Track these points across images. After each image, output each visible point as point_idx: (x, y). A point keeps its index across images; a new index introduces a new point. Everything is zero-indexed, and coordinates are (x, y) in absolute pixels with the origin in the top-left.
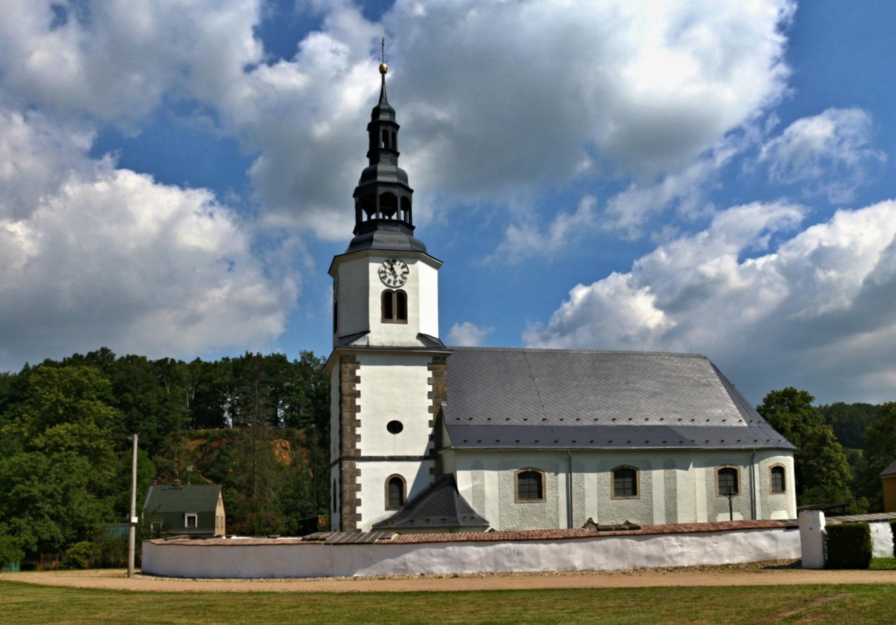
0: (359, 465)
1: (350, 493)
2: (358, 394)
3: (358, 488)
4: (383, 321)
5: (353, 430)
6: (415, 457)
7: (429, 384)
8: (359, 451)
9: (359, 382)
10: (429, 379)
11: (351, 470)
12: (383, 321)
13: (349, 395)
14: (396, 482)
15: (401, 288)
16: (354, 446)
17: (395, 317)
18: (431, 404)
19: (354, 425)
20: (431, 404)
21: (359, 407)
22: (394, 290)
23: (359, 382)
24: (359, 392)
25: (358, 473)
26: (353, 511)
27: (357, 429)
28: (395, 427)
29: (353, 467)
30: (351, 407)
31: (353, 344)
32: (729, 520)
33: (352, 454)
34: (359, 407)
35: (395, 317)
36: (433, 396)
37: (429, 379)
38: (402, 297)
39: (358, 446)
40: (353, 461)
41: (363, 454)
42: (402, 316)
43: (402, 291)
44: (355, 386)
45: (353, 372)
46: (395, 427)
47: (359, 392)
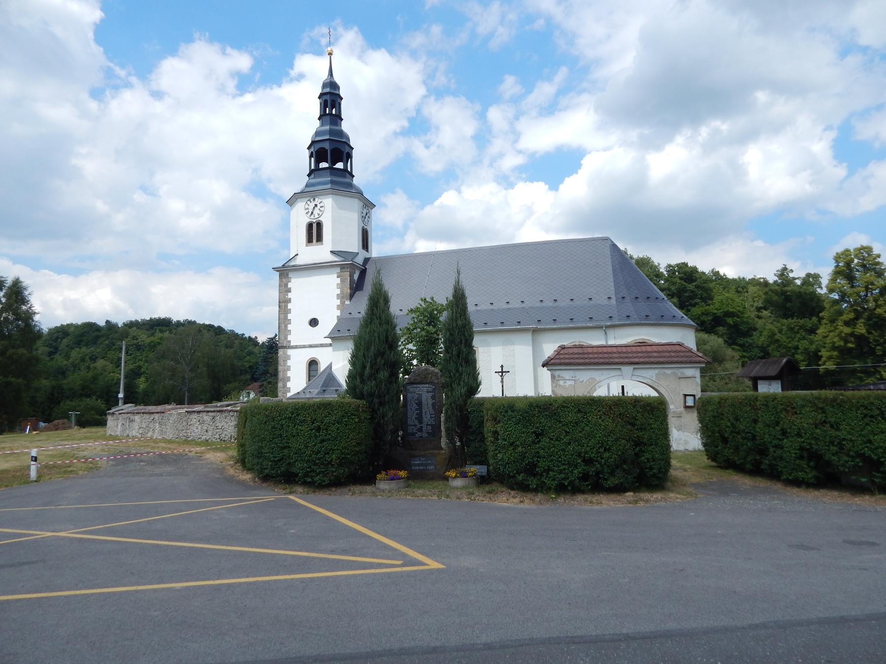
0: (290, 352)
1: (283, 373)
2: (289, 301)
3: (289, 368)
4: (307, 246)
5: (286, 326)
6: (326, 344)
7: (338, 288)
8: (290, 342)
9: (290, 292)
10: (338, 284)
11: (284, 356)
12: (307, 246)
13: (283, 302)
14: (313, 364)
15: (319, 219)
16: (286, 338)
17: (314, 240)
18: (339, 304)
19: (287, 323)
20: (339, 304)
21: (290, 309)
22: (314, 221)
23: (290, 292)
24: (290, 299)
25: (289, 357)
26: (285, 386)
27: (289, 325)
28: (314, 322)
29: (285, 354)
30: (285, 310)
31: (286, 265)
32: (501, 395)
33: (285, 345)
34: (290, 309)
35: (314, 240)
36: (340, 297)
37: (338, 284)
38: (319, 225)
39: (289, 338)
40: (286, 349)
41: (292, 344)
42: (320, 239)
43: (319, 220)
44: (287, 295)
45: (286, 285)
46: (314, 322)
47: (290, 299)
